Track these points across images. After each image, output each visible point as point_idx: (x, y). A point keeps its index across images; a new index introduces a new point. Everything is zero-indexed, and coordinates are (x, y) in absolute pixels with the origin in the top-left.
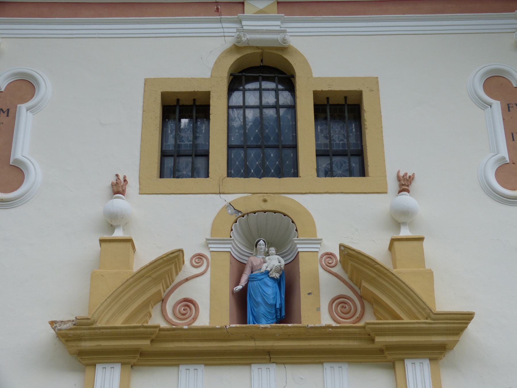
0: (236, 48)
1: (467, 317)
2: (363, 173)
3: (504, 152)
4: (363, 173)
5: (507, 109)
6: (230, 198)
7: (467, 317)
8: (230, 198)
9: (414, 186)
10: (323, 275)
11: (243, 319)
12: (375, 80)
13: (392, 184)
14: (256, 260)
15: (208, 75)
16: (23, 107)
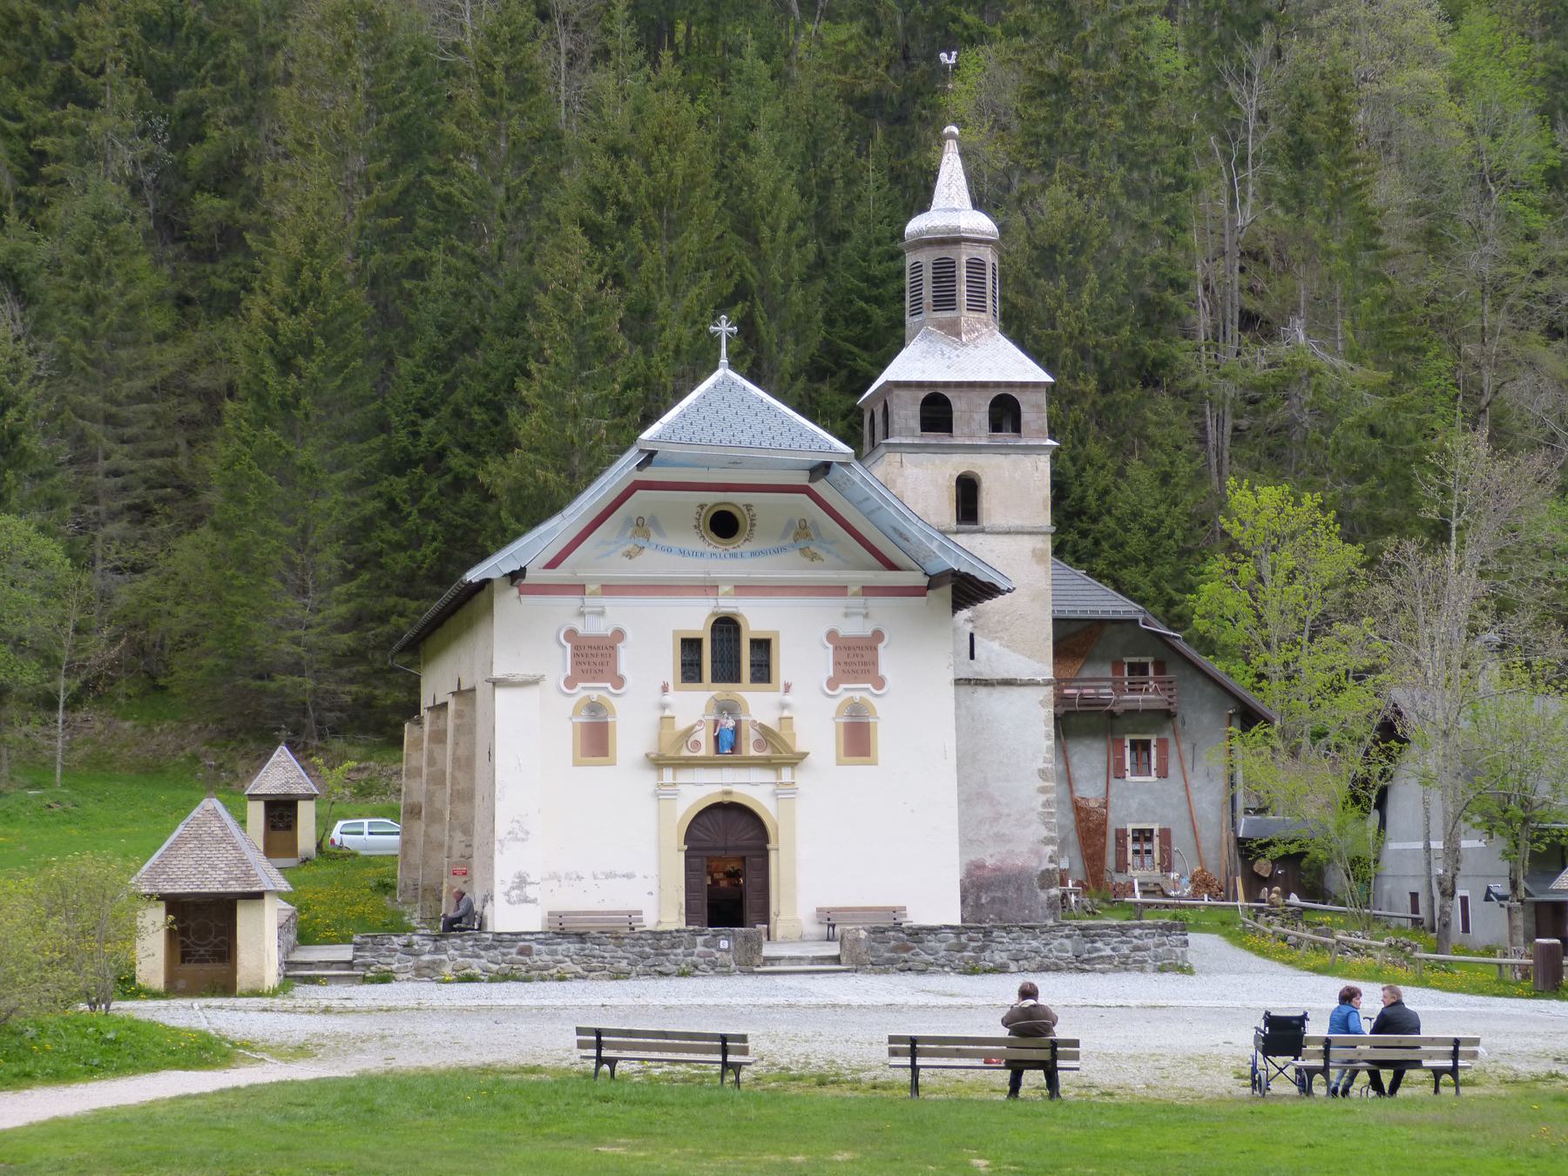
0: (714, 614)
1: (807, 754)
2: (769, 681)
3: (831, 674)
4: (769, 681)
5: (836, 648)
6: (713, 693)
7: (807, 754)
8: (713, 693)
9: (791, 689)
10: (751, 731)
11: (718, 752)
12: (777, 633)
13: (782, 688)
14: (723, 721)
15: (701, 627)
16: (620, 645)
